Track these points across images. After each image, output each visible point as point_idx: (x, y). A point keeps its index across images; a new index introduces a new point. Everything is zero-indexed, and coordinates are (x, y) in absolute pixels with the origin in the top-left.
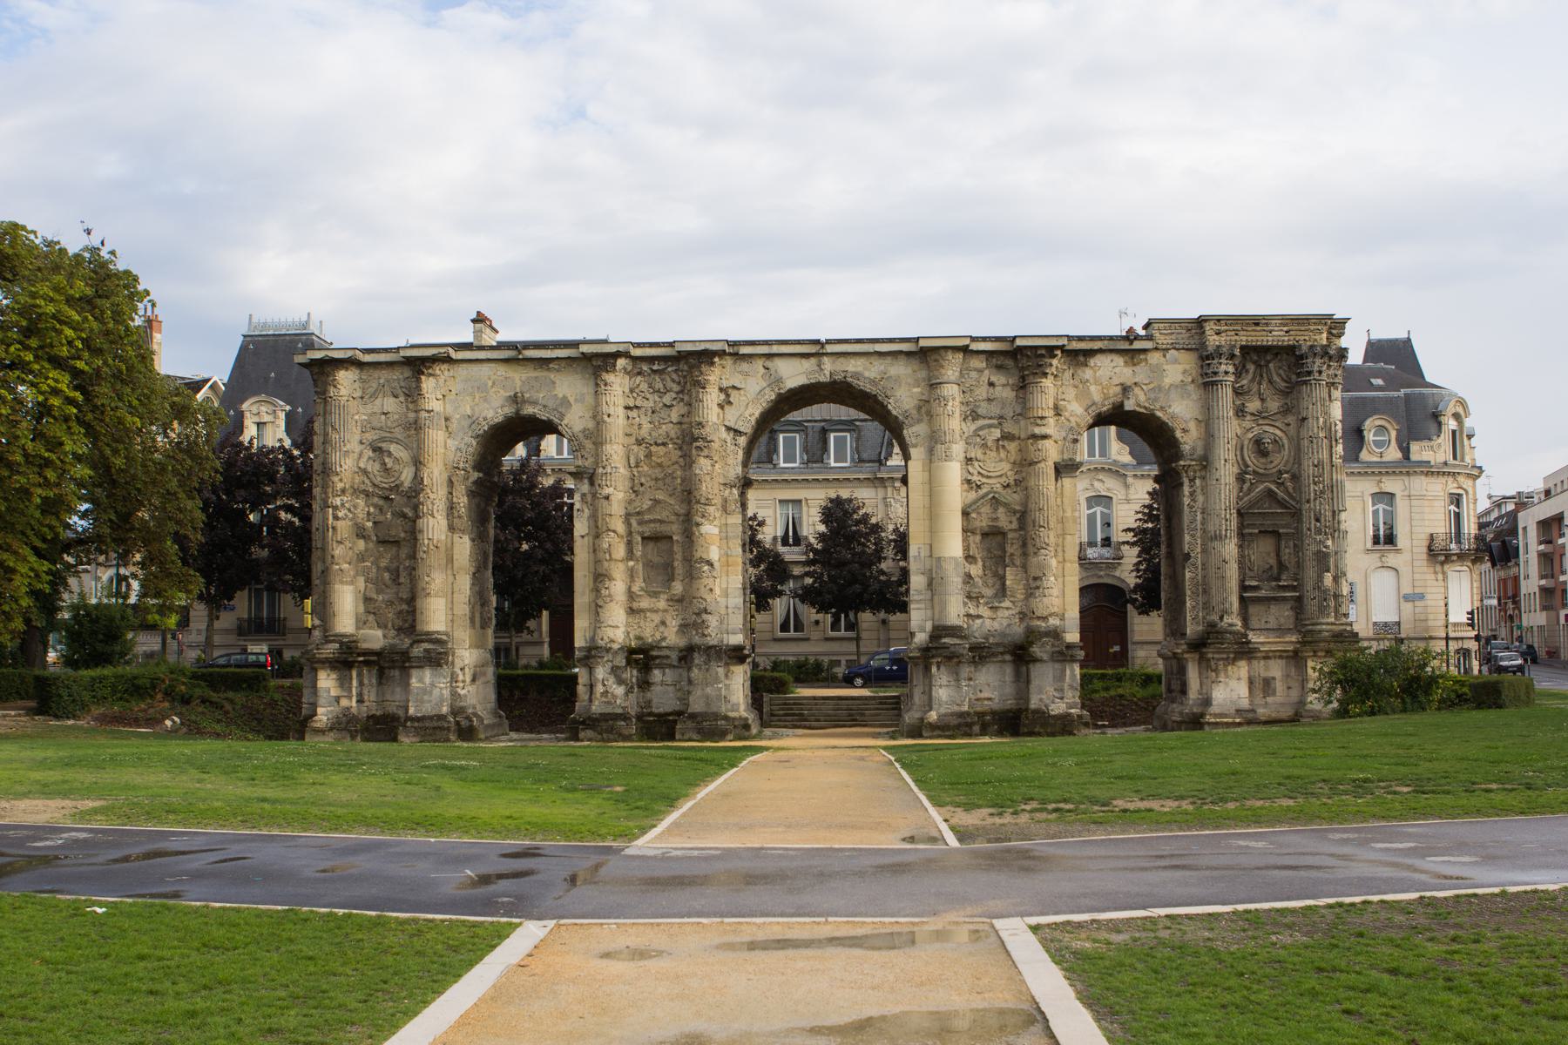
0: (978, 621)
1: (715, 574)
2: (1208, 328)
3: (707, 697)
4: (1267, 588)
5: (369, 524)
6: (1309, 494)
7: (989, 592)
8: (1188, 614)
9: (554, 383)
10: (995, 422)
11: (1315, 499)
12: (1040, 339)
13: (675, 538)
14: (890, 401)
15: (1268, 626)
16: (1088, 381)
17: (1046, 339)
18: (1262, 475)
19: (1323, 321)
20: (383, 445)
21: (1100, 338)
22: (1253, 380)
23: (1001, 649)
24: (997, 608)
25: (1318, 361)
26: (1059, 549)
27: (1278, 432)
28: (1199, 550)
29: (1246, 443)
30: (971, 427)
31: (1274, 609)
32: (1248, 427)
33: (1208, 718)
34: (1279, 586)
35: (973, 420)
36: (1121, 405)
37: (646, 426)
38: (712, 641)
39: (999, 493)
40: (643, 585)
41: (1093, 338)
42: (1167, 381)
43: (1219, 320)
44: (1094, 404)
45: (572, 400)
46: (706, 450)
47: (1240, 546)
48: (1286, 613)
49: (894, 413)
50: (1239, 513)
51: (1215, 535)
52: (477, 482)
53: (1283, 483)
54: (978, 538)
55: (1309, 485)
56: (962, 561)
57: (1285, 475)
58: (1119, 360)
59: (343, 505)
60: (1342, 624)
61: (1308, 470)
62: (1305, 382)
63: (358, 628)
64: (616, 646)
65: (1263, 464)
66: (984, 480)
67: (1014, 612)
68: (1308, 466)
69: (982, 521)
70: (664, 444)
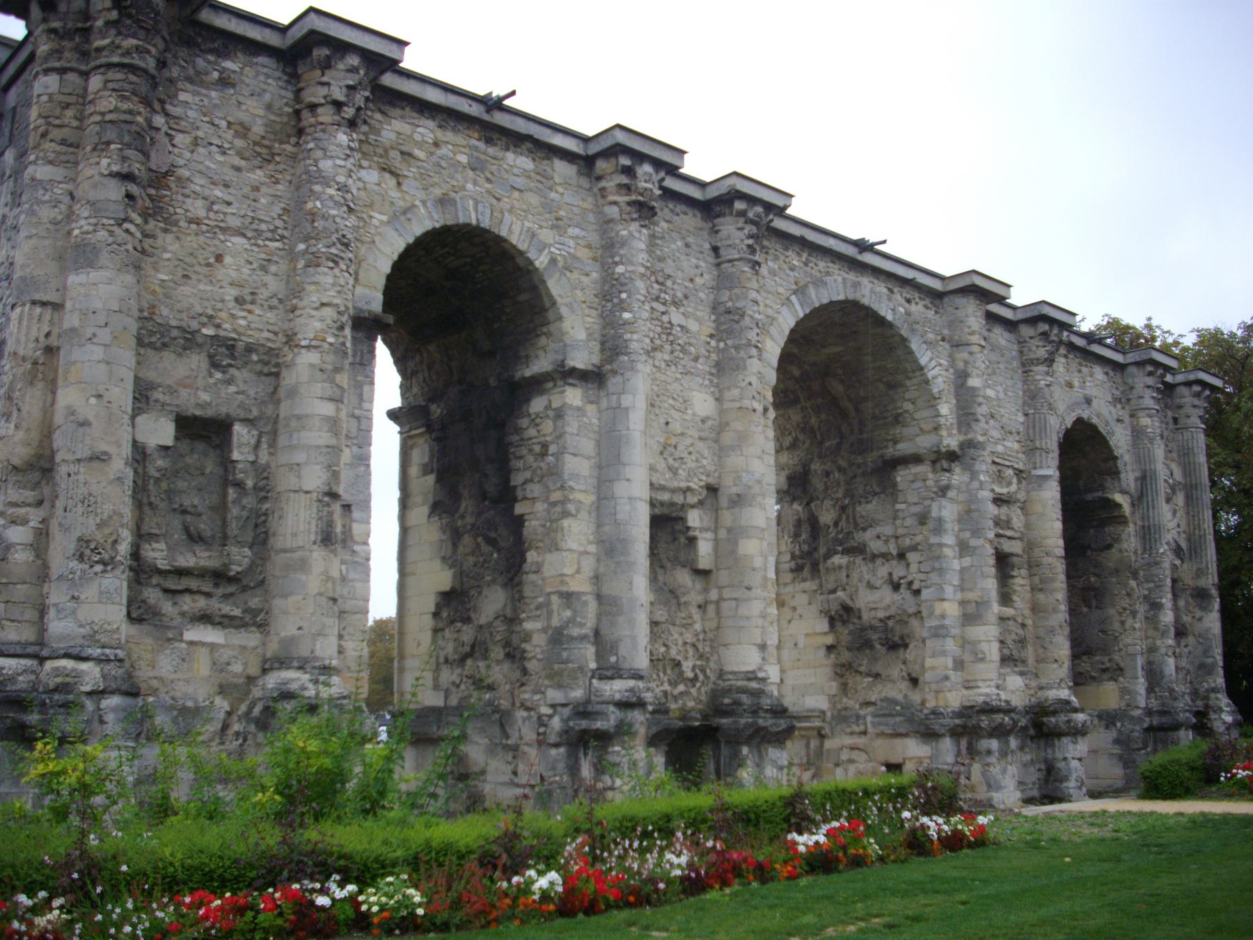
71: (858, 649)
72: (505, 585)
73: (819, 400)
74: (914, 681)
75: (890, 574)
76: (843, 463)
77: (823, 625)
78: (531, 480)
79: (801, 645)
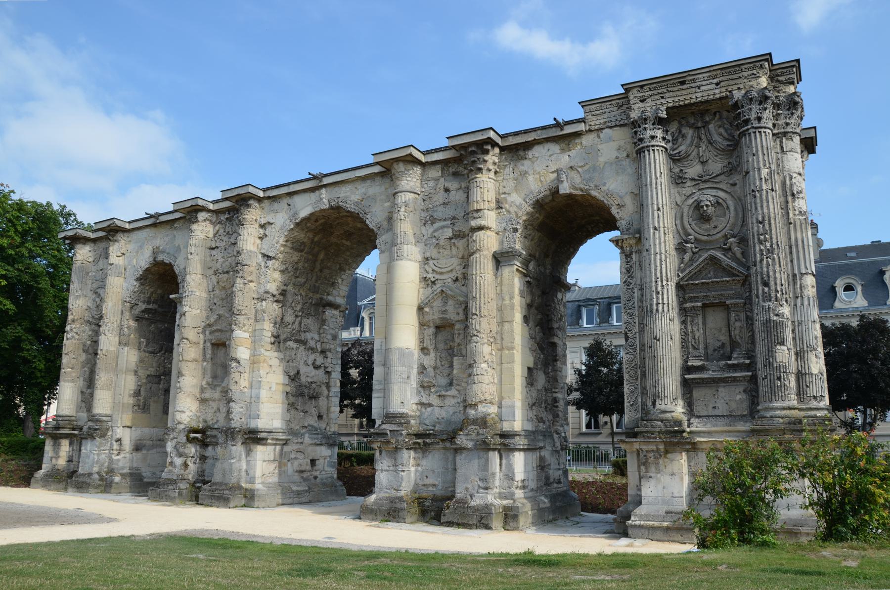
0: (429, 409)
1: (241, 369)
2: (631, 97)
3: (224, 470)
4: (715, 368)
5: (89, 342)
6: (755, 255)
7: (443, 381)
8: (626, 400)
9: (175, 236)
10: (449, 222)
11: (762, 260)
12: (468, 136)
13: (227, 343)
14: (368, 216)
15: (717, 412)
16: (526, 172)
17: (472, 135)
18: (706, 242)
19: (758, 64)
20: (97, 290)
21: (534, 130)
22: (691, 145)
23: (445, 437)
24: (444, 396)
25: (755, 107)
26: (499, 338)
27: (721, 194)
28: (637, 329)
29: (686, 210)
30: (428, 231)
31: (723, 391)
32: (688, 194)
33: (634, 521)
34: (727, 364)
35: (432, 224)
36: (557, 191)
37: (221, 260)
38: (236, 424)
39: (448, 287)
40: (211, 379)
41: (526, 132)
42: (602, 160)
43: (642, 87)
44: (531, 192)
45: (182, 247)
46: (241, 272)
47: (684, 323)
48: (739, 397)
49: (371, 226)
50: (679, 287)
51: (647, 311)
52: (146, 311)
53: (730, 249)
54: (432, 330)
55: (754, 246)
56: (416, 353)
57: (732, 239)
58: (554, 148)
59: (71, 330)
60: (811, 409)
61: (753, 227)
62: (743, 134)
63: (77, 412)
64: (182, 427)
65: (706, 230)
66: (438, 277)
67: (459, 401)
68: (752, 223)
69: (434, 315)
70: (228, 272)
71: (297, 396)
73: (310, 257)
74: (320, 417)
75: (315, 360)
76: (303, 294)
77: (287, 381)
78: (558, 329)
79: (273, 389)
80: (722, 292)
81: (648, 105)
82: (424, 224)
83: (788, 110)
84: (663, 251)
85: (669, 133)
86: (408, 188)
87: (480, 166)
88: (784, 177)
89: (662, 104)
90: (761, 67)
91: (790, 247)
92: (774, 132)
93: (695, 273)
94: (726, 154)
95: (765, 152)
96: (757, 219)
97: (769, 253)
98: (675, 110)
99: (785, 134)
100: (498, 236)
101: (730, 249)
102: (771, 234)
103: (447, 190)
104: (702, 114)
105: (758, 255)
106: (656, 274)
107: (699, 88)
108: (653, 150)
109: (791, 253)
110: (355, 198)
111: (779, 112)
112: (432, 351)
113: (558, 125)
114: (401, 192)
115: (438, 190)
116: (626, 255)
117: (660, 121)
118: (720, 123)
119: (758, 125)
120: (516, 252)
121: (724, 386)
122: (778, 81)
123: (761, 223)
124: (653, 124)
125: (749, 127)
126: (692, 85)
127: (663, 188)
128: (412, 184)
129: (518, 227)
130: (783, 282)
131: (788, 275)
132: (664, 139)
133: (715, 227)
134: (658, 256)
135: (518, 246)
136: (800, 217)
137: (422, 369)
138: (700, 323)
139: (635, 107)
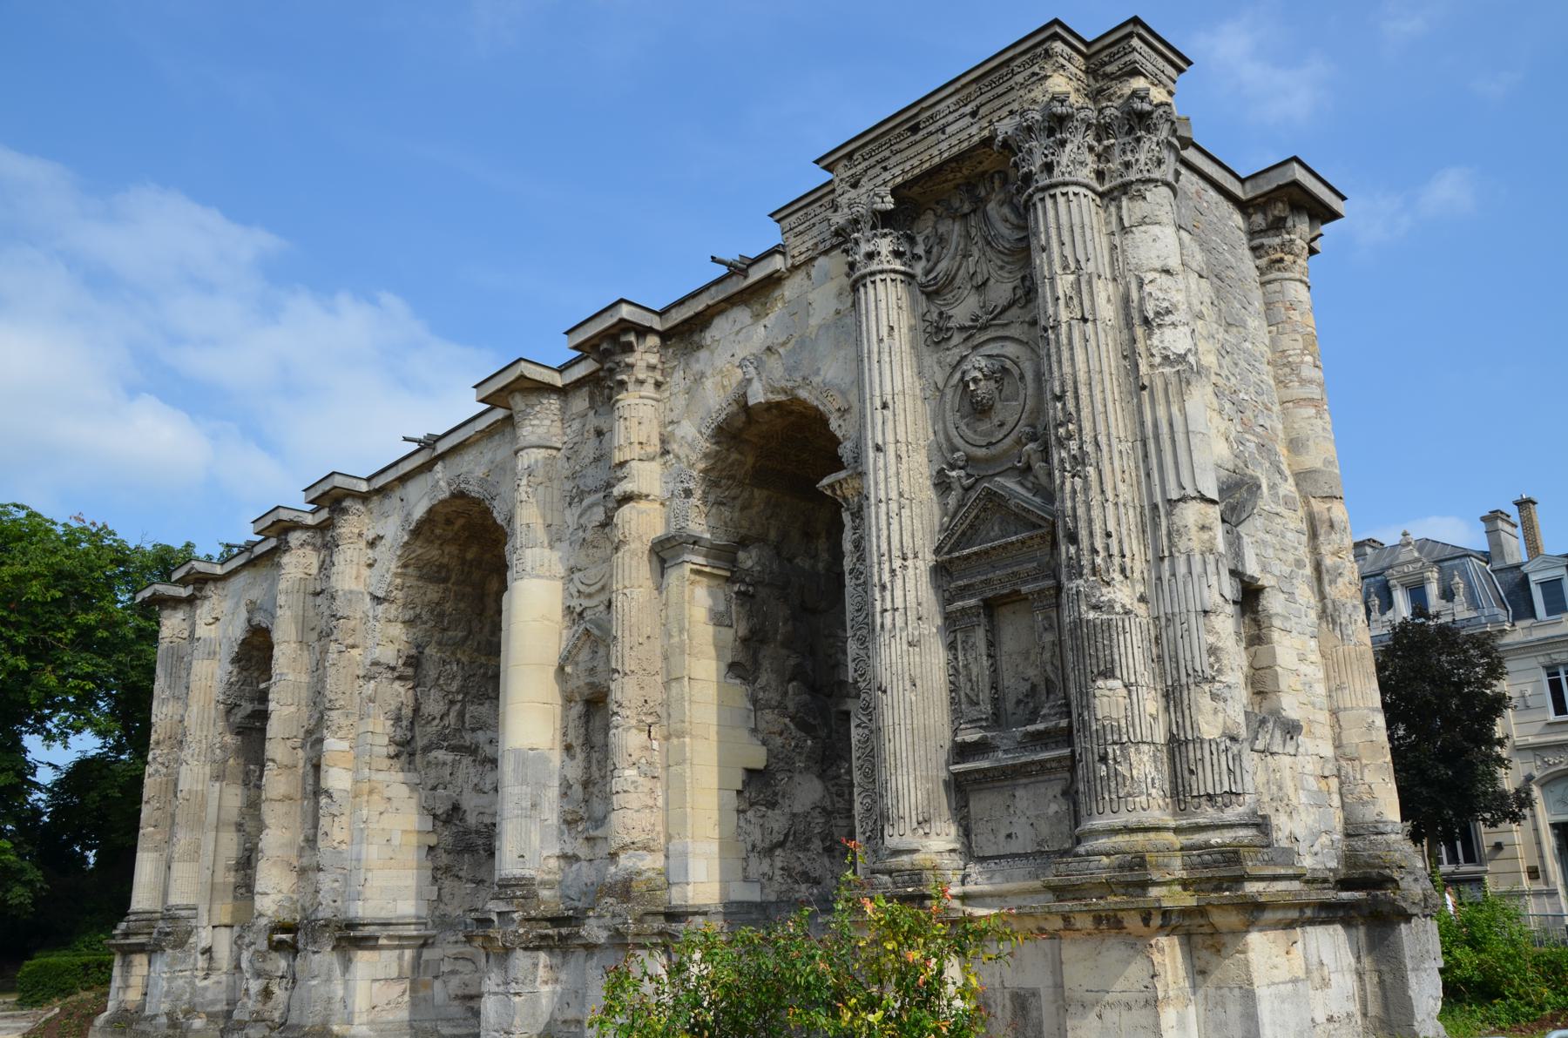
0: (575, 867)
11: (1063, 483)
14: (495, 503)
15: (1015, 847)
17: (598, 320)
18: (987, 461)
19: (1039, 50)
21: (707, 288)
26: (664, 715)
27: (1010, 349)
30: (571, 516)
31: (1024, 798)
32: (955, 363)
34: (1027, 734)
35: (581, 501)
36: (746, 403)
42: (814, 321)
43: (849, 156)
47: (951, 647)
54: (578, 709)
56: (556, 757)
57: (1031, 446)
58: (741, 315)
66: (586, 603)
69: (580, 681)
72: (821, 776)
80: (1015, 569)
81: (863, 190)
82: (570, 504)
83: (1131, 131)
84: (894, 495)
85: (920, 239)
86: (533, 439)
87: (619, 377)
88: (1127, 286)
89: (885, 183)
90: (1048, 55)
91: (1144, 444)
92: (1100, 189)
93: (964, 533)
94: (1019, 260)
95: (1066, 238)
96: (1052, 390)
97: (1077, 464)
98: (916, 189)
99: (1125, 188)
100: (664, 510)
101: (1028, 468)
102: (1079, 420)
103: (599, 433)
104: (970, 186)
105: (1057, 473)
106: (879, 547)
107: (944, 133)
108: (873, 282)
109: (1146, 456)
110: (480, 472)
111: (1106, 143)
112: (578, 750)
113: (737, 269)
114: (522, 449)
115: (586, 435)
116: (852, 514)
117: (884, 220)
118: (1002, 196)
119: (1047, 182)
120: (681, 536)
121: (1026, 785)
122: (1106, 76)
123: (1060, 398)
124: (874, 227)
125: (1030, 190)
126: (932, 128)
127: (896, 359)
128: (541, 430)
129: (692, 485)
130: (1111, 527)
131: (1142, 507)
132: (897, 254)
133: (1002, 425)
134: (883, 506)
135: (698, 526)
136: (1167, 370)
137: (566, 787)
138: (982, 646)
139: (843, 200)
